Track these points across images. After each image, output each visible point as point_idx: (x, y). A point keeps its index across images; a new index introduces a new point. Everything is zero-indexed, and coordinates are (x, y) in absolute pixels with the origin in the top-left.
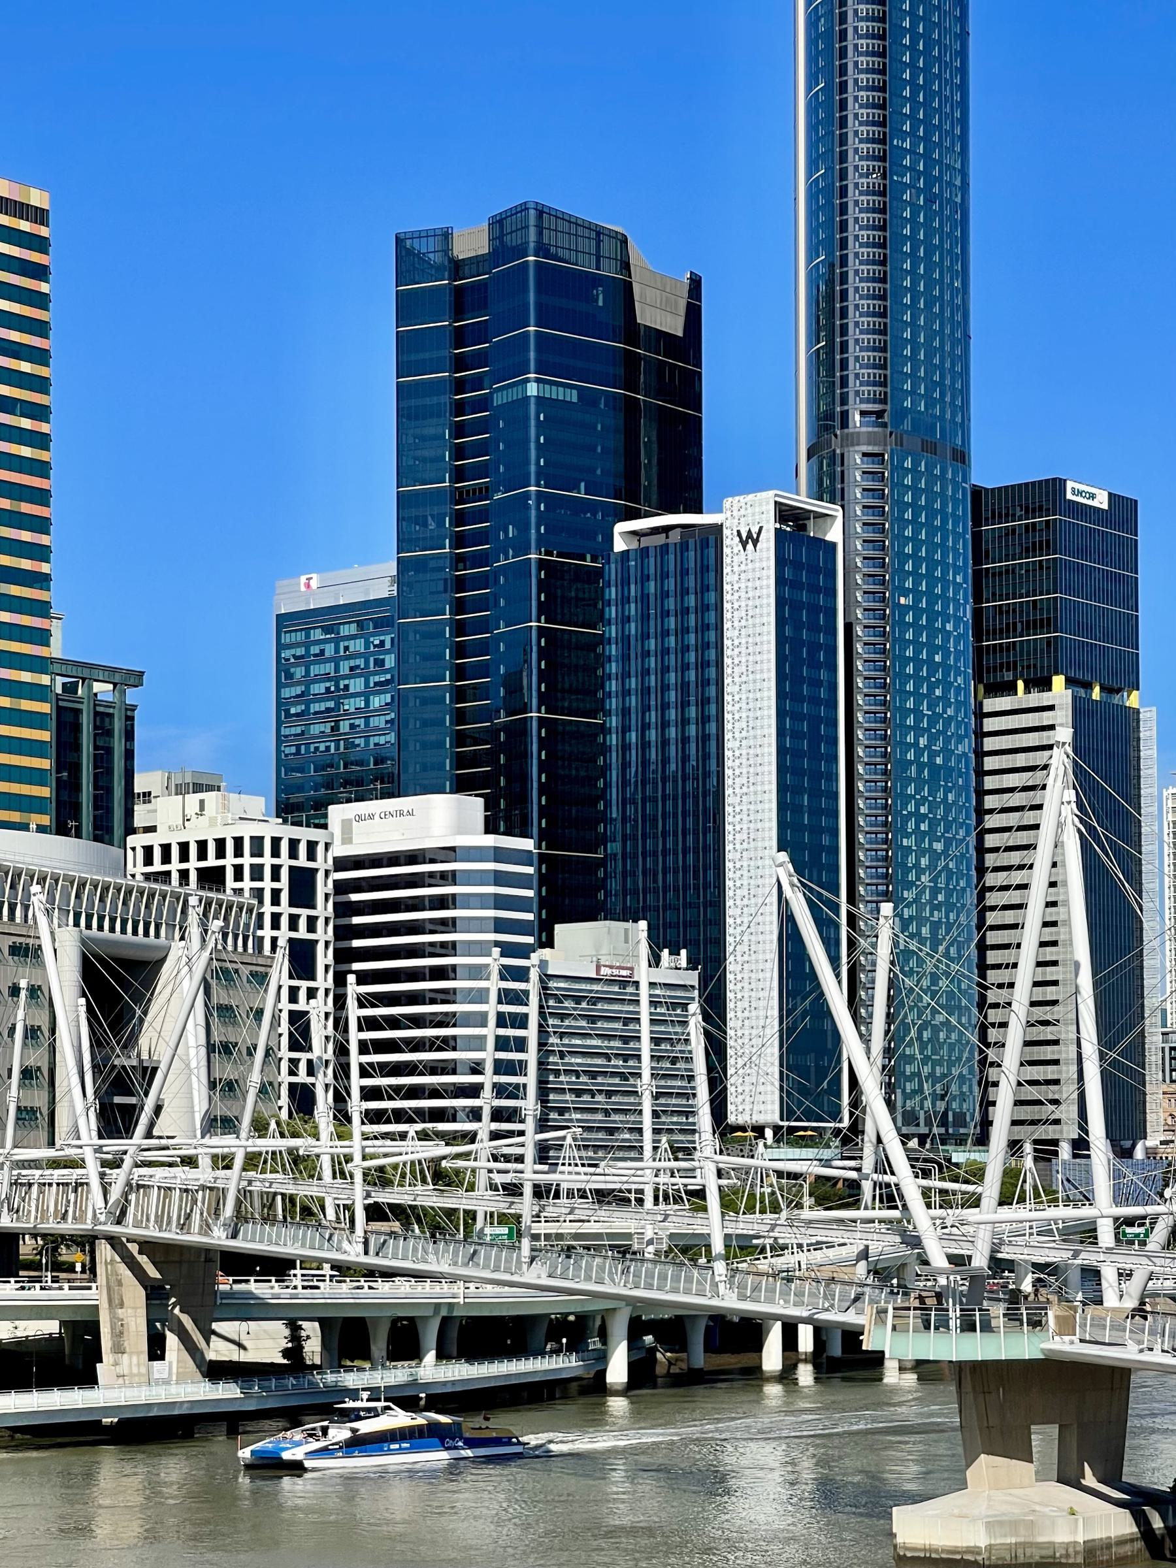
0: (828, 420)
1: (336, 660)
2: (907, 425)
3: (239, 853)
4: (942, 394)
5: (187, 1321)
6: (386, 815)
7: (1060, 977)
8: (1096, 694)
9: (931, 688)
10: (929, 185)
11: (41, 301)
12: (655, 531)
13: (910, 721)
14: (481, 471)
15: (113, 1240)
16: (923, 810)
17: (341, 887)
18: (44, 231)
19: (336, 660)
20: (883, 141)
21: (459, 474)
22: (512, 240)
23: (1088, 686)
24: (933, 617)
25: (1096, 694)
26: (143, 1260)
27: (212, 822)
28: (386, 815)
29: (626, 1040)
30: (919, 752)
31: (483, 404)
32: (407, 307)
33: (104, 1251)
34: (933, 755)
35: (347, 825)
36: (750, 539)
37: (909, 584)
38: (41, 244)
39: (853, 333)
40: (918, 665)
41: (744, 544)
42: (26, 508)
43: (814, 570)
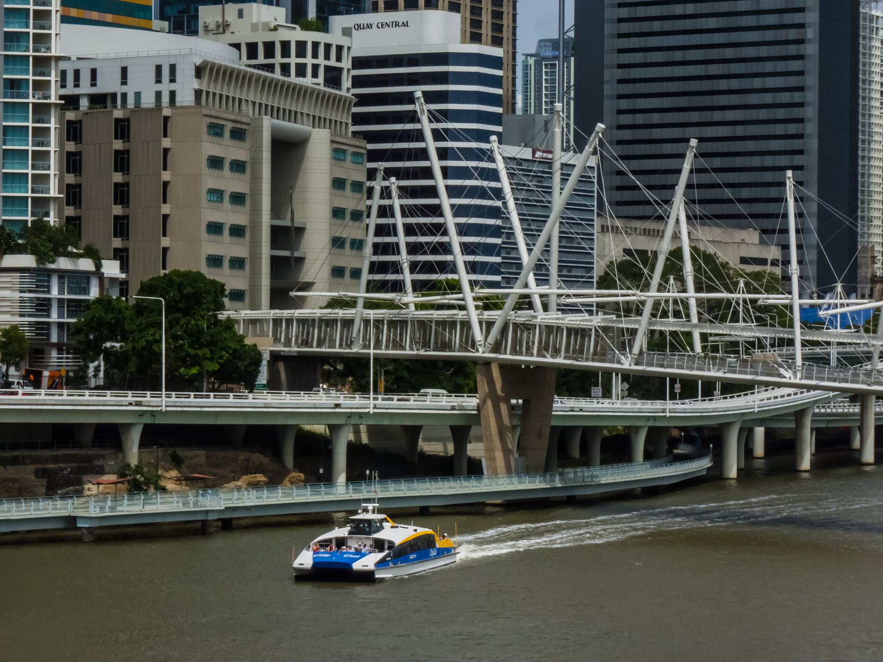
6: (383, 25)
7: (805, 164)
17: (358, 82)
28: (383, 25)
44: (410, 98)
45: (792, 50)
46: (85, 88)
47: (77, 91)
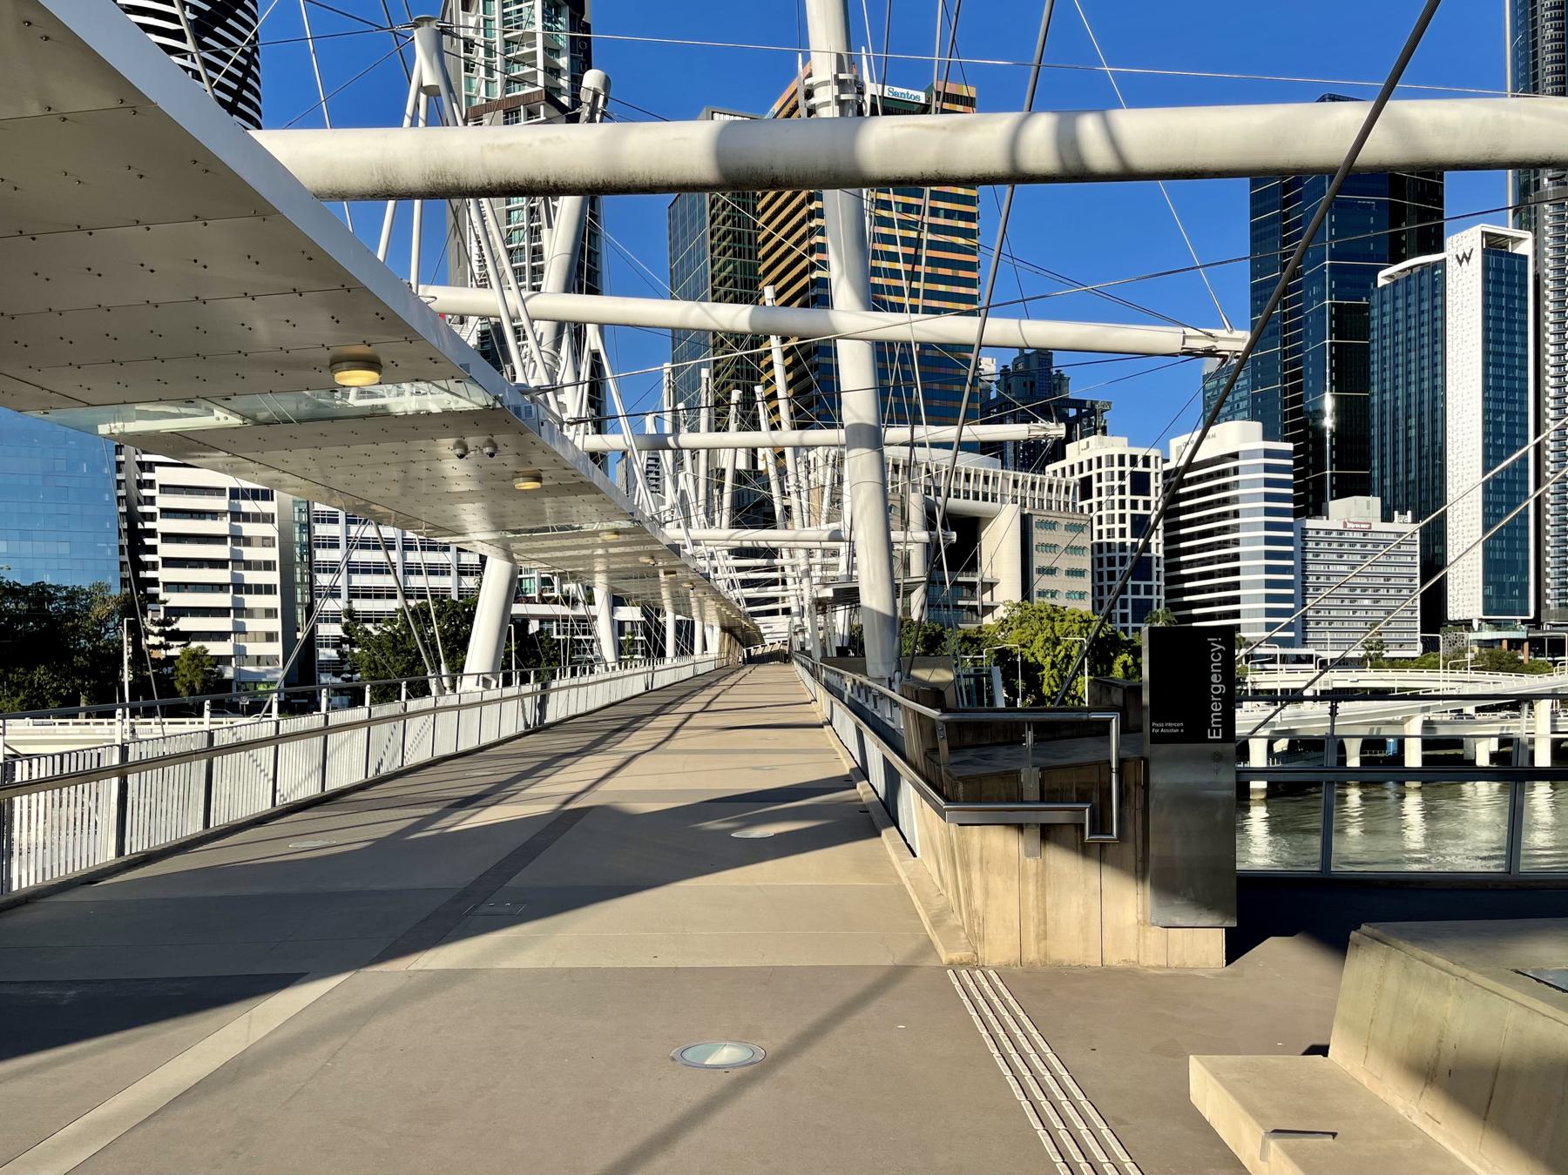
3: (1099, 466)
41: (1461, 262)
42: (962, 274)
43: (1511, 272)
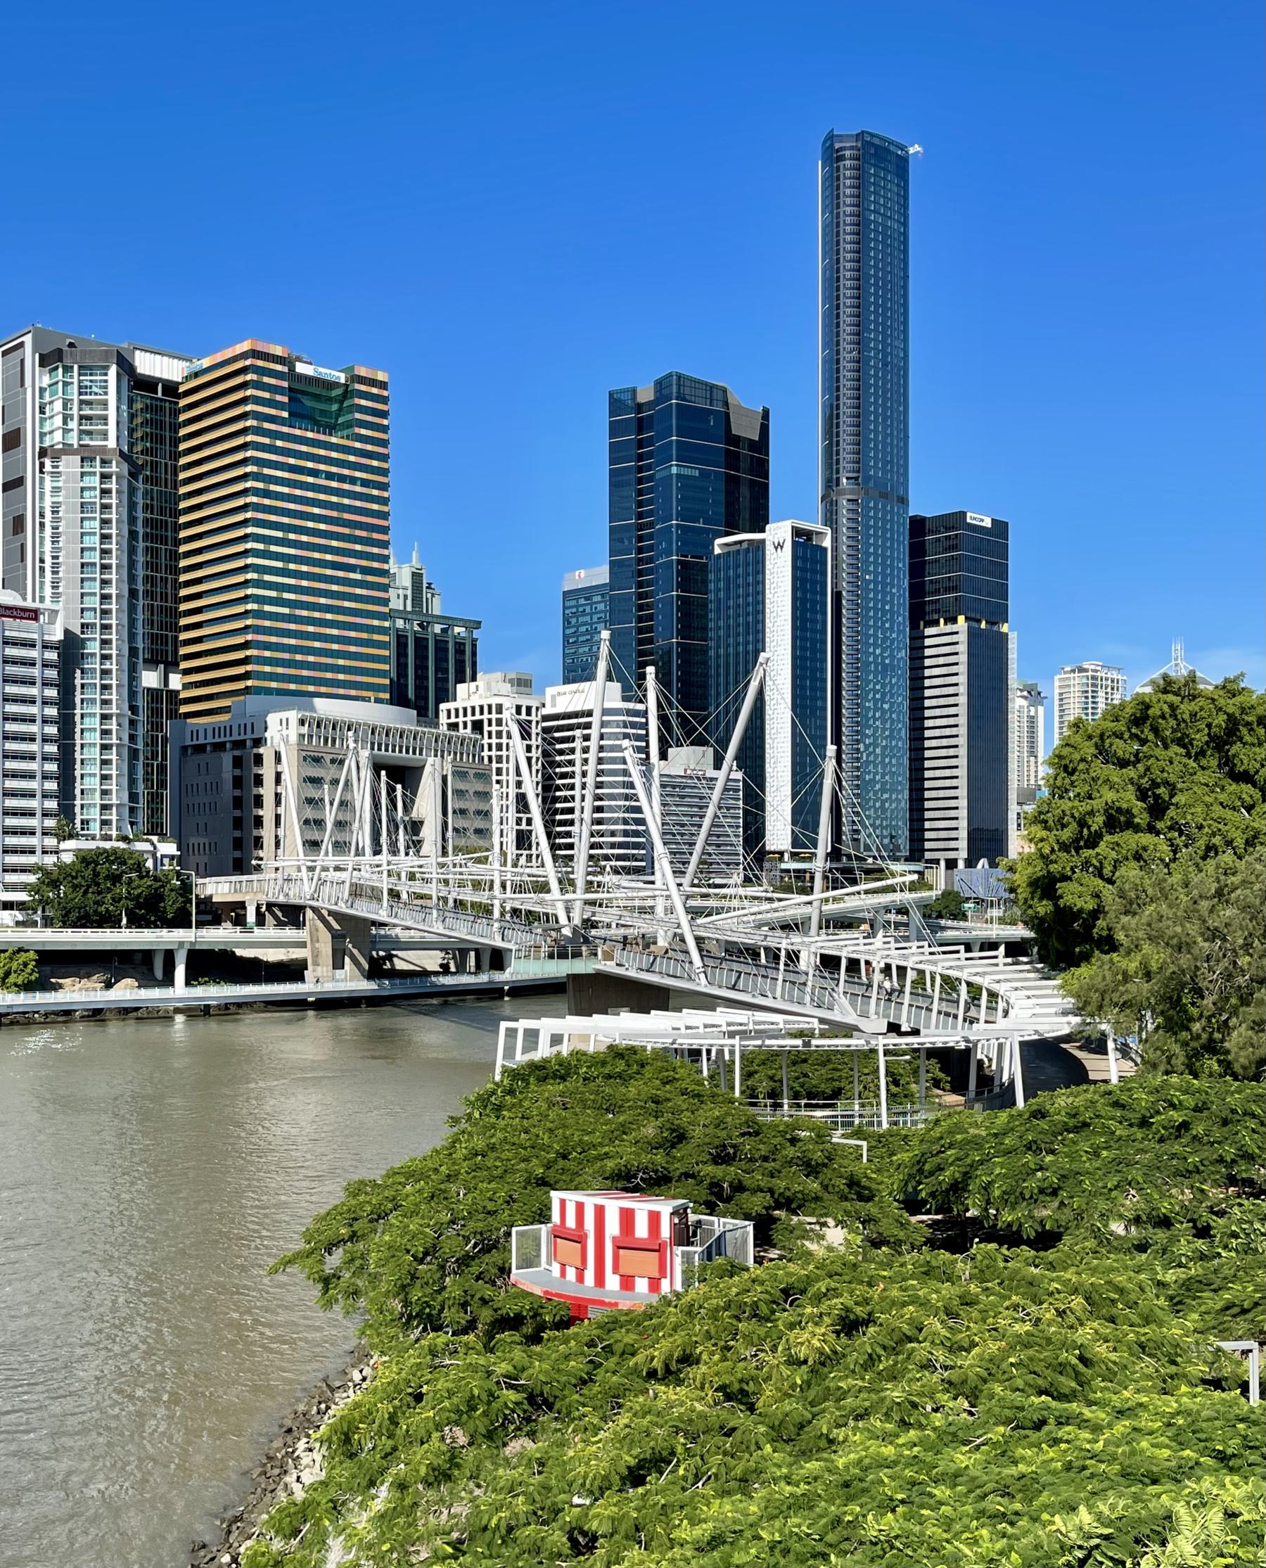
0: (831, 483)
1: (591, 614)
2: (871, 484)
3: (490, 713)
4: (892, 468)
5: (355, 952)
8: (983, 625)
9: (883, 624)
10: (885, 357)
11: (384, 429)
12: (736, 543)
13: (871, 641)
14: (650, 513)
15: (314, 909)
16: (878, 687)
17: (546, 730)
18: (385, 393)
19: (591, 614)
20: (858, 334)
21: (640, 516)
22: (665, 392)
23: (979, 621)
24: (884, 585)
25: (983, 625)
26: (330, 919)
27: (481, 697)
29: (701, 807)
30: (876, 657)
31: (650, 478)
32: (615, 429)
33: (309, 914)
34: (884, 658)
35: (553, 697)
36: (779, 546)
37: (871, 568)
38: (384, 400)
39: (842, 436)
40: (875, 609)
42: (375, 536)
43: (814, 562)
44: (572, 739)
45: (951, 701)
46: (249, 735)
47: (242, 737)
